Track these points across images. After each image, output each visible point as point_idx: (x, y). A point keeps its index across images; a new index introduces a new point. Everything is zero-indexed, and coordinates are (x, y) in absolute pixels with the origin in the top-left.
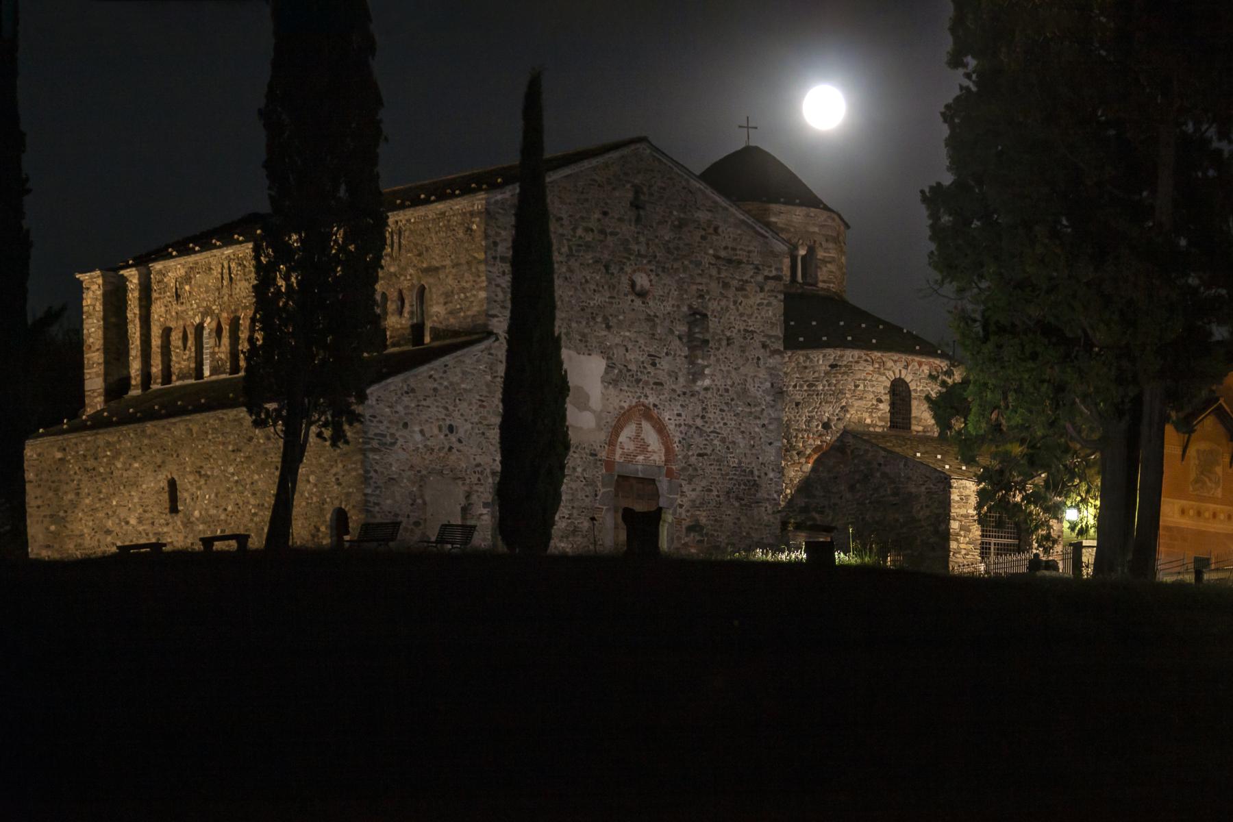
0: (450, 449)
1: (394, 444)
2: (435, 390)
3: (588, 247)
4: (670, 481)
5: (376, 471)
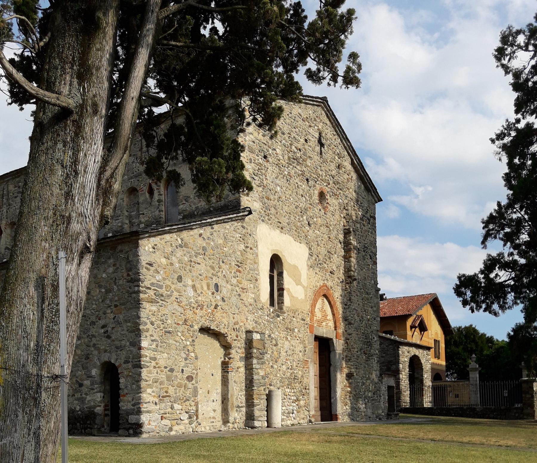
0: (216, 307)
1: (169, 296)
2: (204, 249)
5: (152, 323)
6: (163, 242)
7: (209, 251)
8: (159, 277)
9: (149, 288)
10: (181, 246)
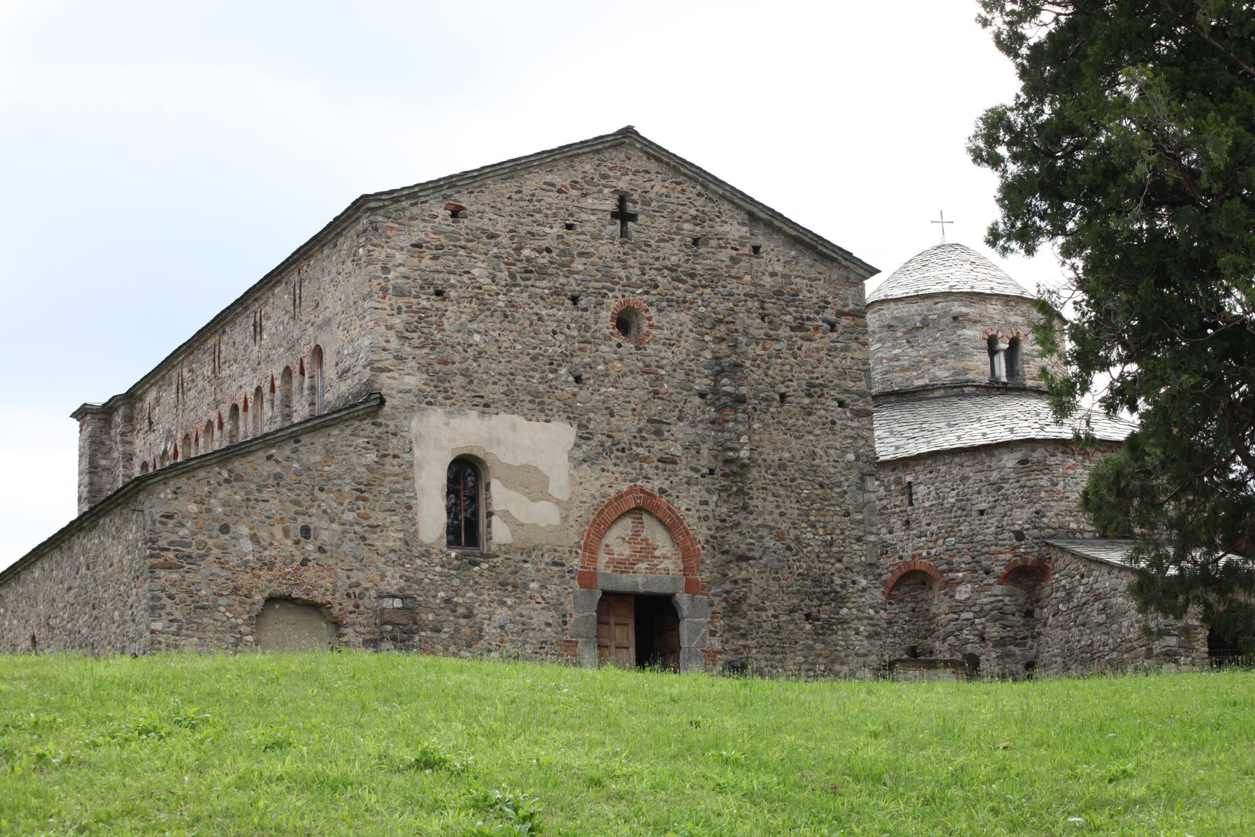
1: (203, 557)
2: (278, 477)
3: (542, 273)
4: (692, 599)
5: (171, 597)
6: (192, 482)
7: (289, 478)
8: (183, 532)
9: (167, 550)
10: (227, 481)
